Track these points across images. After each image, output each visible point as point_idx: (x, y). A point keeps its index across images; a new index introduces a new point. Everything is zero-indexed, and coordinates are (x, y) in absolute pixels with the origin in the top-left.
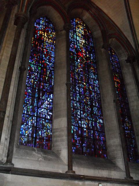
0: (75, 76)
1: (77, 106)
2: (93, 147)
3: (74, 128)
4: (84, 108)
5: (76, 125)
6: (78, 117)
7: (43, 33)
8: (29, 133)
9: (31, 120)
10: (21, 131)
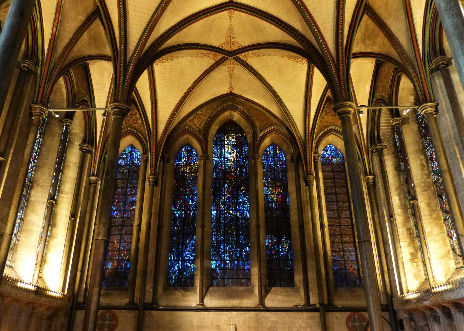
0: (220, 207)
1: (220, 240)
6: (221, 251)
8: (176, 276)
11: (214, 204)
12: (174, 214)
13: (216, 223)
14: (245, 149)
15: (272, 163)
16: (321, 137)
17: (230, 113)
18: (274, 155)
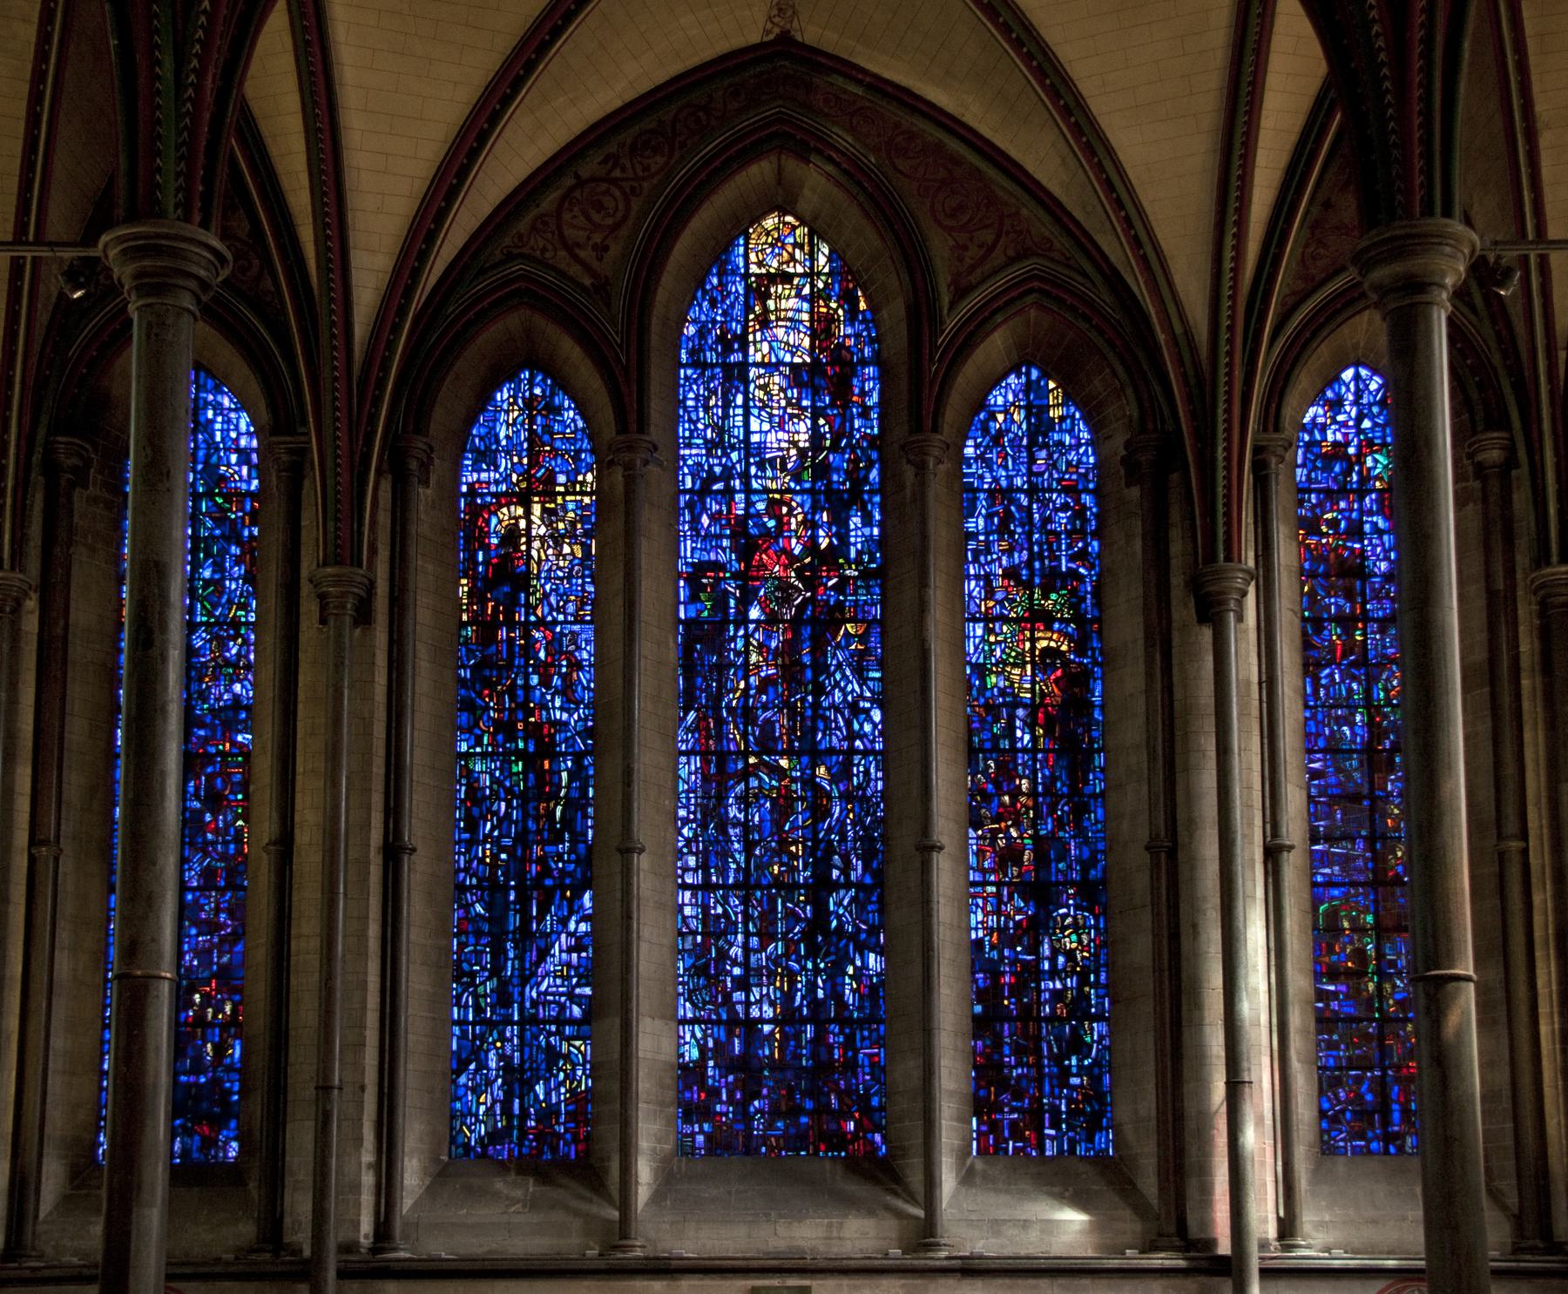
0: (720, 736)
1: (726, 914)
2: (809, 1104)
3: (704, 1031)
4: (769, 915)
5: (718, 1014)
7: (520, 511)
8: (494, 1101)
9: (499, 1044)
10: (459, 1099)
11: (692, 716)
12: (468, 773)
13: (704, 825)
15: (1018, 482)
16: (1304, 326)
18: (1032, 434)
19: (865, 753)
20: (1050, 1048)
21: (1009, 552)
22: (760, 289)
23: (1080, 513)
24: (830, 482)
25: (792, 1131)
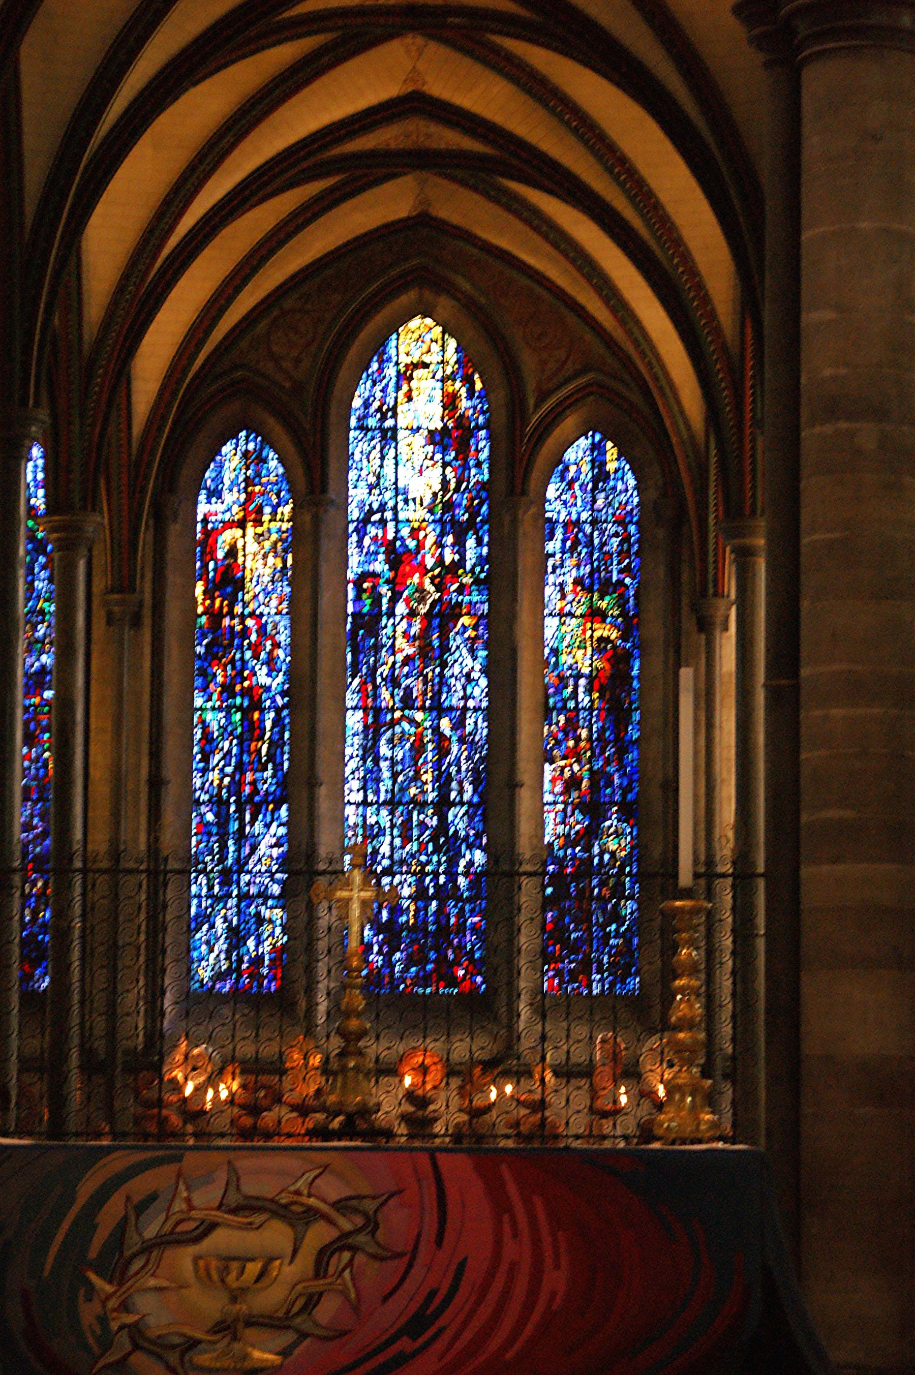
0: (376, 696)
1: (377, 822)
4: (407, 826)
7: (238, 532)
11: (357, 681)
12: (203, 721)
13: (364, 759)
14: (477, 451)
17: (421, 296)
18: (595, 480)
19: (476, 710)
20: (597, 919)
21: (578, 566)
22: (404, 377)
23: (626, 538)
24: (453, 516)
25: (421, 974)
